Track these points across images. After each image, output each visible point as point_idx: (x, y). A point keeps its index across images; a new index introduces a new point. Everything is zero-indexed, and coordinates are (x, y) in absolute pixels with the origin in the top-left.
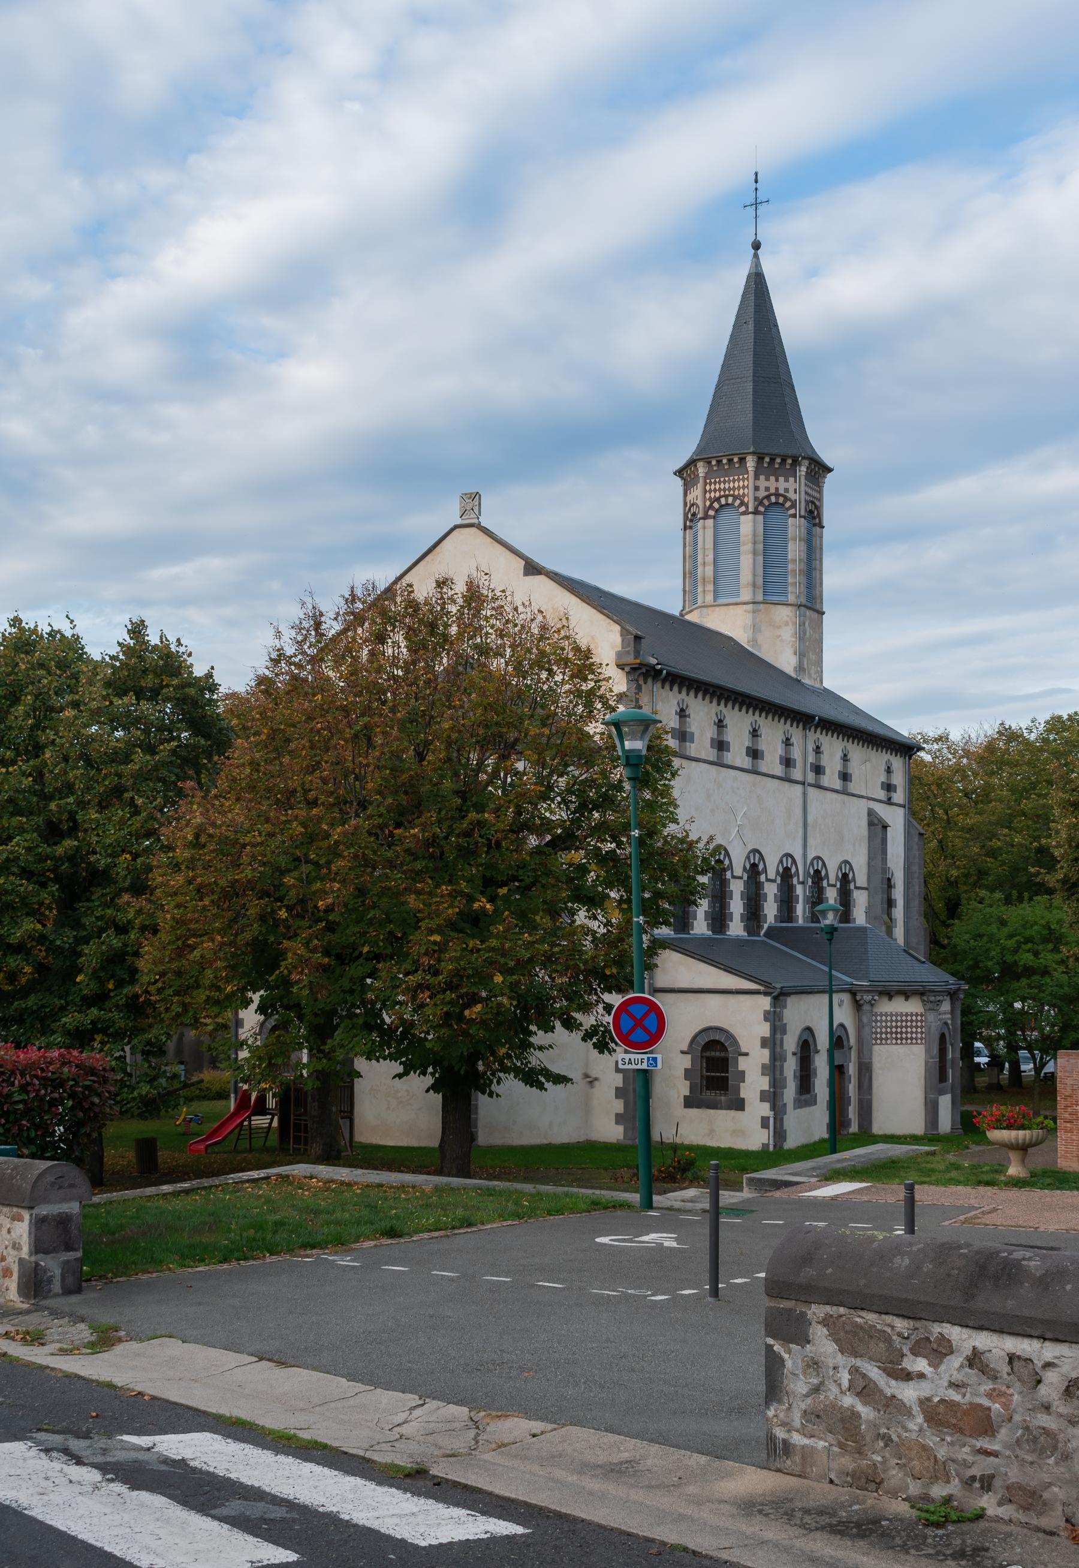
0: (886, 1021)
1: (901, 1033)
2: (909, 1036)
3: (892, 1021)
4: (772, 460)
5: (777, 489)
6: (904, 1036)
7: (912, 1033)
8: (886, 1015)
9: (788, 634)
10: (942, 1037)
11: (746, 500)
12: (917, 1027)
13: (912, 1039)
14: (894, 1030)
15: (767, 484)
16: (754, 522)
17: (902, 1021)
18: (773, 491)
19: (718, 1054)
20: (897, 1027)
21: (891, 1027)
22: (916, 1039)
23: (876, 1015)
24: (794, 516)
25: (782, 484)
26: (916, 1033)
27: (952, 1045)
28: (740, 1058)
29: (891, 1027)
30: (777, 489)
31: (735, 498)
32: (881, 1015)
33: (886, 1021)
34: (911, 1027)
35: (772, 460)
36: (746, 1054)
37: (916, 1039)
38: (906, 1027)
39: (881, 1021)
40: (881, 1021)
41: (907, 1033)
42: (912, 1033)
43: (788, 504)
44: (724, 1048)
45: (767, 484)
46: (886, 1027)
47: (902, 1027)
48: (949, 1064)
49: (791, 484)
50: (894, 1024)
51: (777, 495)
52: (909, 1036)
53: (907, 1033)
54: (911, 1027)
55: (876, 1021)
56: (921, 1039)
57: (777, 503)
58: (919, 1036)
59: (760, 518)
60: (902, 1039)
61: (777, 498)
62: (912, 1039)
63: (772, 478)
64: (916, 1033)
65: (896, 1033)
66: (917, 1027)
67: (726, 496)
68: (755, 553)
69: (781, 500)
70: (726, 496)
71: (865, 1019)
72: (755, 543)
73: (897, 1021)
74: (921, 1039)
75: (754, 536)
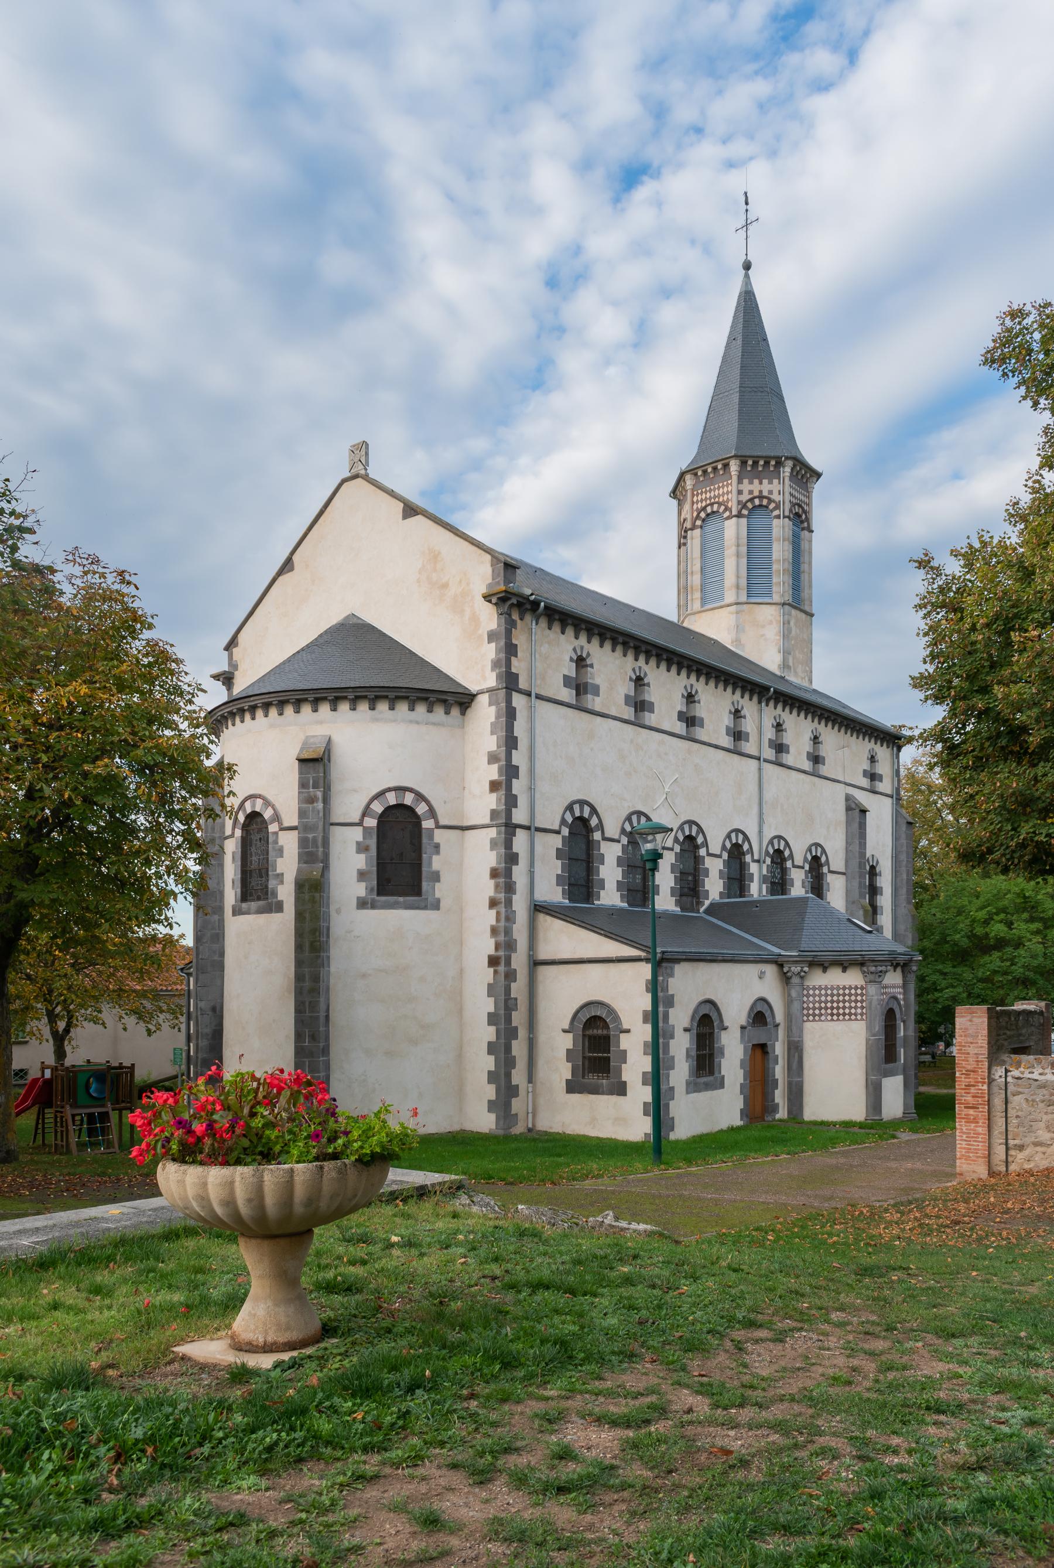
0: (820, 995)
1: (838, 1008)
6: (841, 1011)
10: (890, 1016)
13: (850, 1014)
14: (829, 1005)
20: (832, 1002)
21: (826, 1002)
32: (814, 988)
39: (814, 995)
40: (814, 995)
41: (844, 1008)
47: (838, 1002)
52: (847, 1011)
53: (844, 1008)
60: (838, 1015)
62: (850, 1014)
65: (832, 1008)
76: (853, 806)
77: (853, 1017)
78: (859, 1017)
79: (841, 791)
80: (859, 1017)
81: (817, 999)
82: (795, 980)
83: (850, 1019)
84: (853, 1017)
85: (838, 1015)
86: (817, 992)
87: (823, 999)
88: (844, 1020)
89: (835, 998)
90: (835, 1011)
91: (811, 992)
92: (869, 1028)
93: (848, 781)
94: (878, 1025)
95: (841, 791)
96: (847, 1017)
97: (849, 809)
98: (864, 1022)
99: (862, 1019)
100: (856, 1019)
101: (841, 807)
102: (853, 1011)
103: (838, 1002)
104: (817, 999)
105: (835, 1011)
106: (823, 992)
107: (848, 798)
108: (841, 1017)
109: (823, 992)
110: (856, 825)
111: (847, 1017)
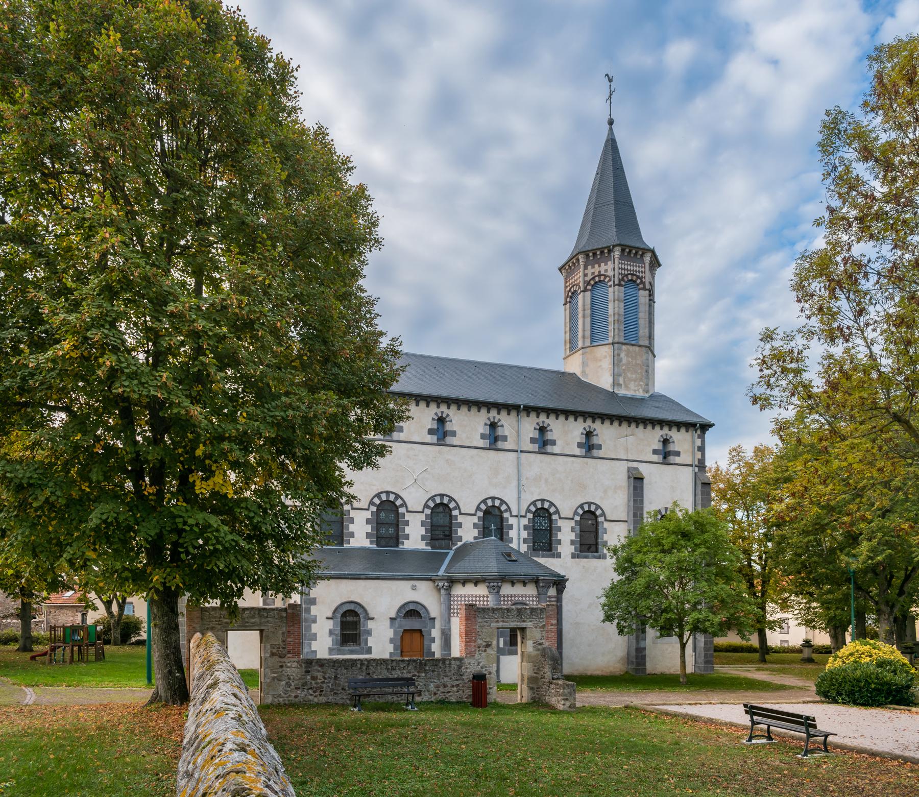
4: (595, 254)
5: (600, 272)
8: (461, 596)
9: (607, 364)
15: (593, 270)
18: (597, 273)
19: (352, 619)
28: (369, 621)
35: (595, 254)
36: (373, 619)
44: (356, 614)
45: (593, 270)
51: (599, 275)
57: (600, 281)
61: (600, 278)
63: (596, 266)
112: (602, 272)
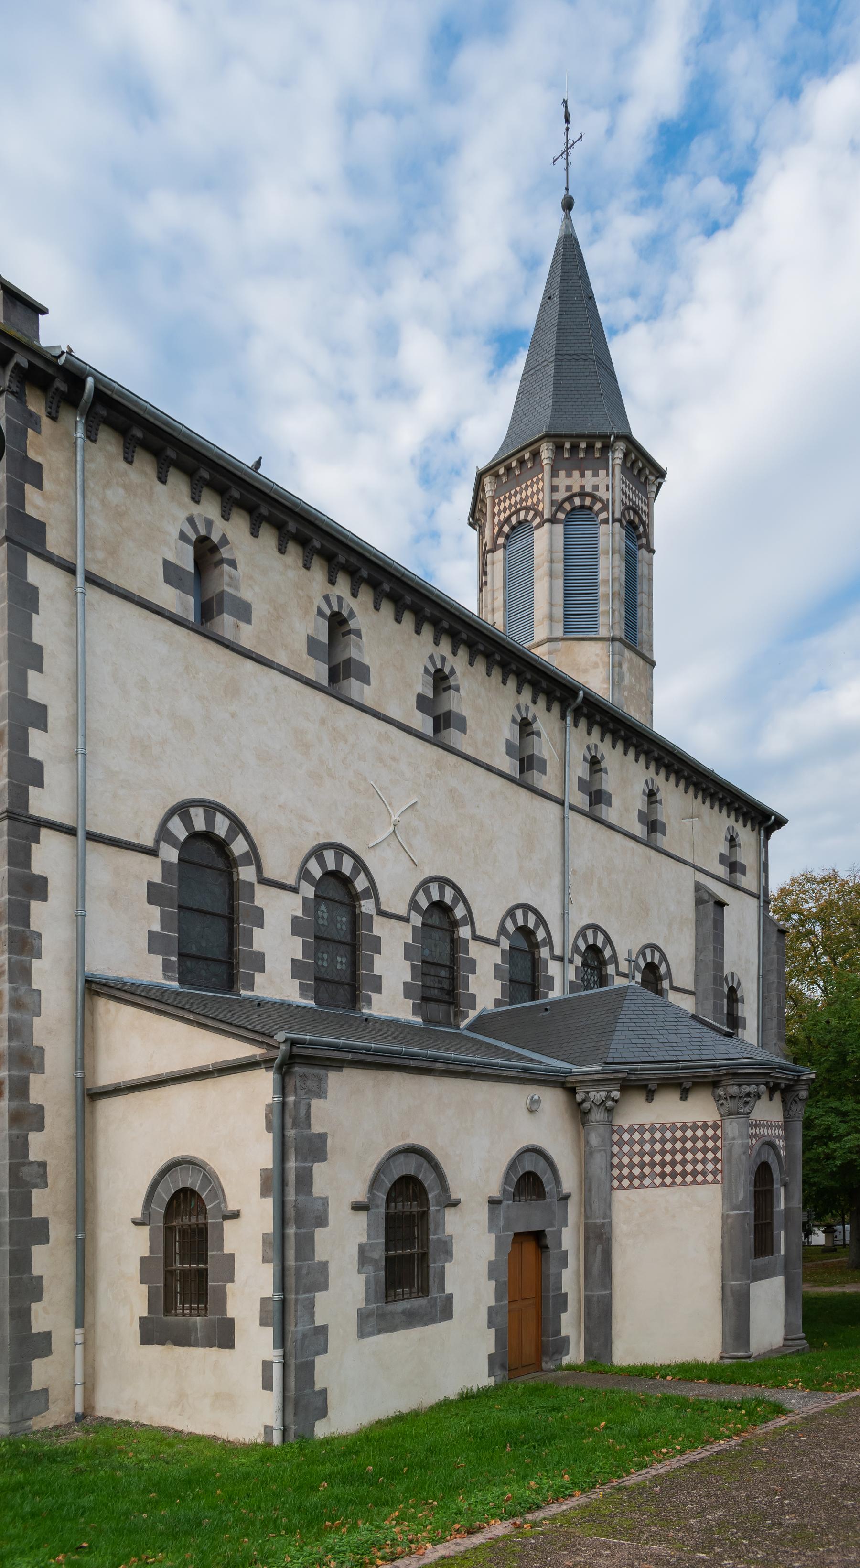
0: (642, 1142)
1: (673, 1163)
2: (689, 1168)
3: (653, 1141)
5: (582, 487)
6: (679, 1168)
7: (695, 1162)
11: (540, 508)
12: (705, 1150)
13: (694, 1173)
14: (658, 1158)
16: (551, 533)
17: (674, 1140)
20: (663, 1152)
21: (652, 1153)
22: (704, 1173)
23: (621, 1130)
24: (605, 521)
25: (589, 481)
26: (704, 1161)
27: (785, 1185)
29: (652, 1153)
30: (582, 487)
31: (527, 509)
33: (642, 1142)
34: (694, 1150)
37: (704, 1173)
38: (684, 1151)
39: (631, 1143)
40: (631, 1143)
41: (684, 1162)
42: (695, 1162)
43: (597, 506)
46: (642, 1154)
47: (673, 1152)
48: (778, 1220)
49: (602, 480)
50: (658, 1147)
52: (689, 1168)
53: (684, 1162)
54: (694, 1150)
55: (621, 1143)
56: (715, 1173)
57: (582, 507)
58: (710, 1167)
59: (559, 528)
62: (694, 1173)
64: (704, 1161)
65: (663, 1164)
66: (705, 1150)
67: (517, 512)
68: (551, 575)
69: (588, 501)
70: (517, 512)
71: (594, 1140)
72: (552, 562)
73: (663, 1141)
74: (715, 1173)
75: (551, 551)
76: (706, 897)
77: (700, 1178)
78: (710, 1178)
79: (689, 878)
80: (710, 1178)
81: (637, 1148)
82: (597, 1116)
83: (694, 1182)
84: (700, 1178)
85: (673, 1175)
86: (637, 1136)
87: (647, 1147)
88: (684, 1183)
89: (668, 1146)
90: (668, 1169)
91: (626, 1137)
92: (727, 1196)
93: (698, 864)
94: (743, 1192)
95: (689, 878)
96: (689, 1179)
97: (699, 902)
98: (718, 1187)
99: (715, 1182)
100: (705, 1182)
101: (689, 899)
102: (700, 1167)
103: (673, 1152)
104: (637, 1148)
105: (668, 1169)
106: (647, 1136)
107: (698, 887)
108: (679, 1179)
109: (647, 1136)
110: (710, 923)
111: (689, 1179)
112: (588, 489)
